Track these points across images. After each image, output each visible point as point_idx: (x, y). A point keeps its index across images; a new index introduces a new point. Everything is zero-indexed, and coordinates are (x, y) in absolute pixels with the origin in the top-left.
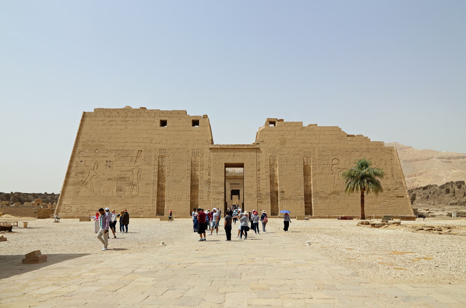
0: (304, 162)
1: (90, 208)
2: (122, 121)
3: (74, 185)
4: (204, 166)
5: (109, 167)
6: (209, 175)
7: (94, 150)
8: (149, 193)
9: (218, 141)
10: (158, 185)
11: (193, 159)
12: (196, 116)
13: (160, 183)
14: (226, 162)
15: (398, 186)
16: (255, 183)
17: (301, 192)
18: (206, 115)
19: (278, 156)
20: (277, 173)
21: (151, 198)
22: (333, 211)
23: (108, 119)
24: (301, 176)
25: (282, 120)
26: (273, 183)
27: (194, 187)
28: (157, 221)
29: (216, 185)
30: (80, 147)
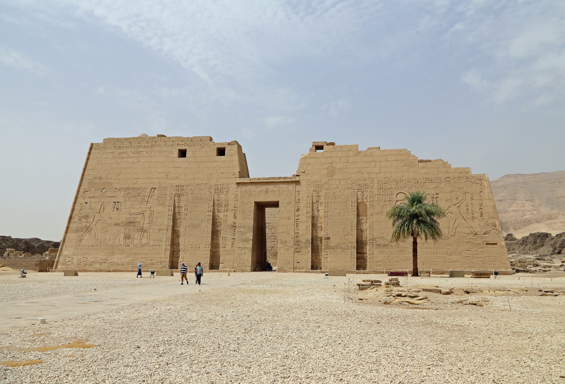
1: (92, 260)
2: (134, 153)
3: (77, 231)
5: (117, 209)
6: (235, 217)
7: (101, 189)
8: (161, 241)
11: (216, 198)
12: (221, 144)
13: (176, 228)
15: (489, 228)
16: (292, 227)
19: (324, 191)
20: (321, 213)
21: (164, 247)
22: (395, 264)
23: (120, 151)
25: (333, 144)
27: (215, 233)
29: (242, 230)
30: (85, 186)
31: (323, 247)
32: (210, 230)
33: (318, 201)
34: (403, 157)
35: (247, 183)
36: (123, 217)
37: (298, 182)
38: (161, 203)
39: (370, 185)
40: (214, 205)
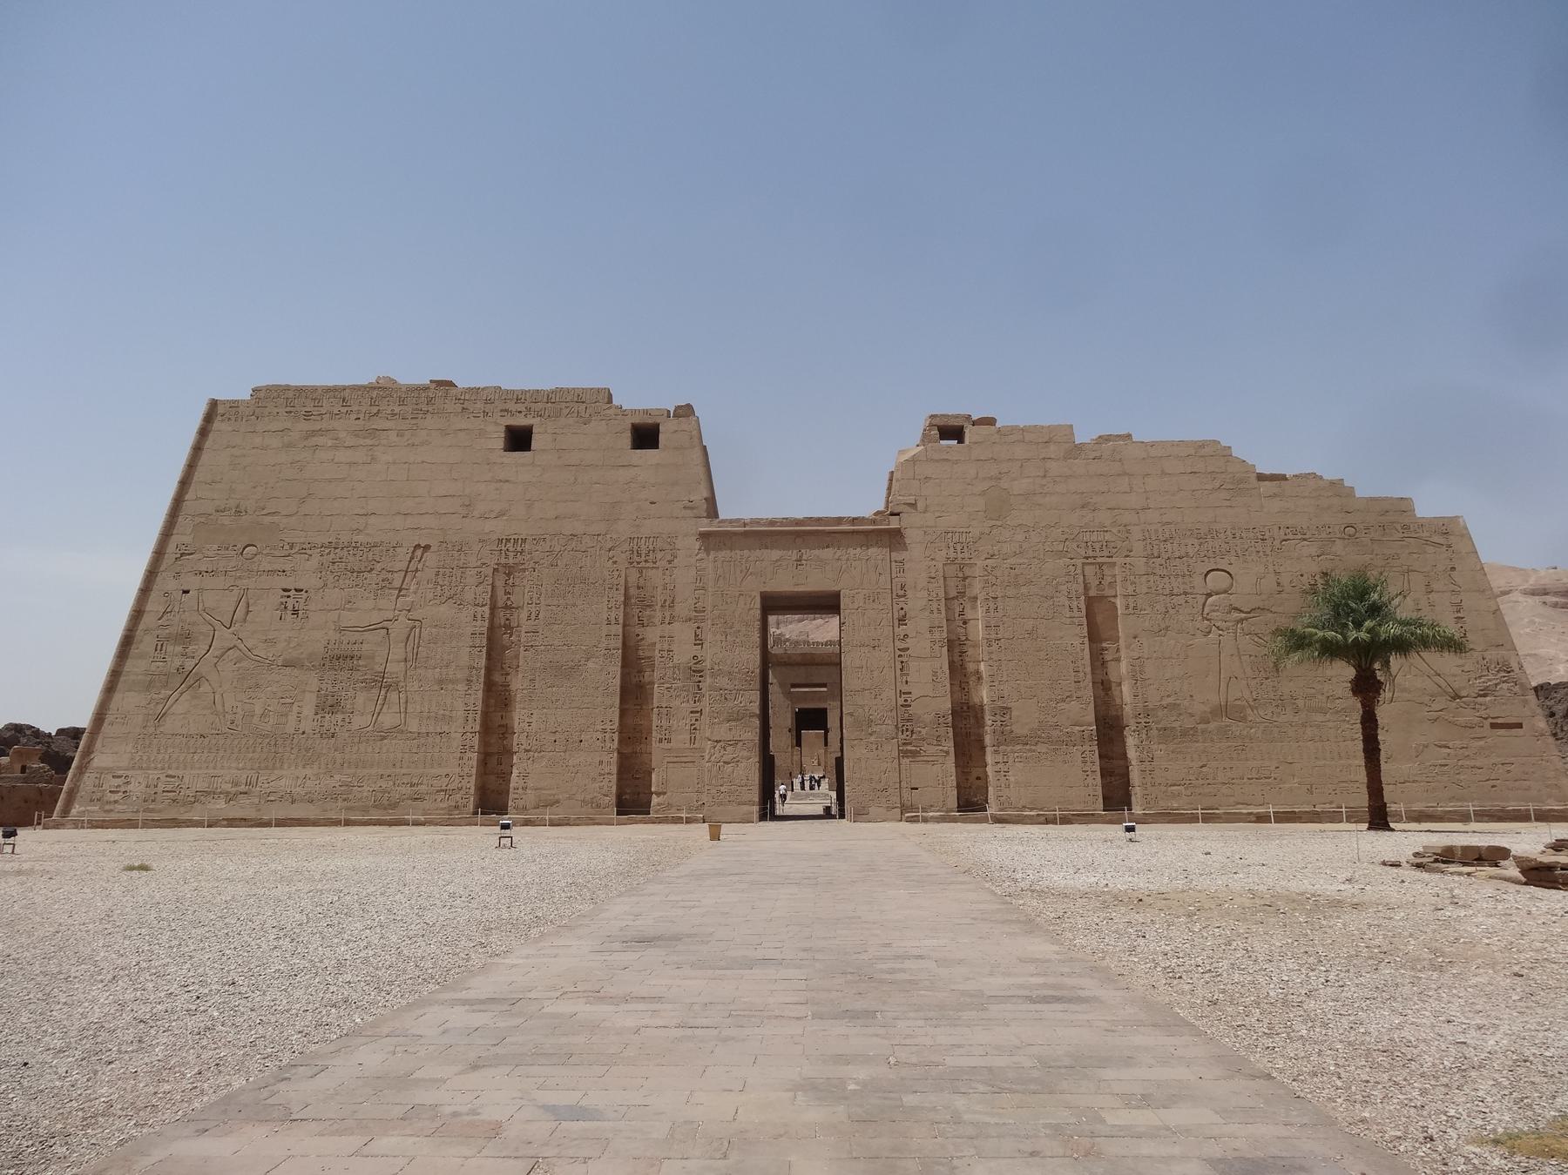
0: (1086, 588)
2: (356, 434)
3: (149, 687)
4: (678, 607)
5: (295, 612)
6: (699, 642)
9: (736, 507)
10: (489, 686)
11: (633, 579)
12: (646, 412)
13: (497, 678)
14: (768, 589)
15: (1491, 679)
17: (1082, 712)
18: (689, 406)
20: (978, 630)
22: (1224, 790)
23: (304, 426)
24: (1074, 638)
25: (990, 421)
26: (960, 673)
27: (634, 694)
28: (483, 836)
31: (988, 740)
32: (618, 681)
33: (962, 594)
34: (1210, 462)
35: (735, 533)
36: (316, 636)
37: (894, 539)
38: (447, 594)
39: (1119, 544)
40: (626, 603)
